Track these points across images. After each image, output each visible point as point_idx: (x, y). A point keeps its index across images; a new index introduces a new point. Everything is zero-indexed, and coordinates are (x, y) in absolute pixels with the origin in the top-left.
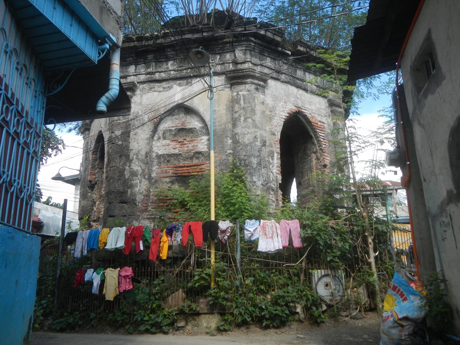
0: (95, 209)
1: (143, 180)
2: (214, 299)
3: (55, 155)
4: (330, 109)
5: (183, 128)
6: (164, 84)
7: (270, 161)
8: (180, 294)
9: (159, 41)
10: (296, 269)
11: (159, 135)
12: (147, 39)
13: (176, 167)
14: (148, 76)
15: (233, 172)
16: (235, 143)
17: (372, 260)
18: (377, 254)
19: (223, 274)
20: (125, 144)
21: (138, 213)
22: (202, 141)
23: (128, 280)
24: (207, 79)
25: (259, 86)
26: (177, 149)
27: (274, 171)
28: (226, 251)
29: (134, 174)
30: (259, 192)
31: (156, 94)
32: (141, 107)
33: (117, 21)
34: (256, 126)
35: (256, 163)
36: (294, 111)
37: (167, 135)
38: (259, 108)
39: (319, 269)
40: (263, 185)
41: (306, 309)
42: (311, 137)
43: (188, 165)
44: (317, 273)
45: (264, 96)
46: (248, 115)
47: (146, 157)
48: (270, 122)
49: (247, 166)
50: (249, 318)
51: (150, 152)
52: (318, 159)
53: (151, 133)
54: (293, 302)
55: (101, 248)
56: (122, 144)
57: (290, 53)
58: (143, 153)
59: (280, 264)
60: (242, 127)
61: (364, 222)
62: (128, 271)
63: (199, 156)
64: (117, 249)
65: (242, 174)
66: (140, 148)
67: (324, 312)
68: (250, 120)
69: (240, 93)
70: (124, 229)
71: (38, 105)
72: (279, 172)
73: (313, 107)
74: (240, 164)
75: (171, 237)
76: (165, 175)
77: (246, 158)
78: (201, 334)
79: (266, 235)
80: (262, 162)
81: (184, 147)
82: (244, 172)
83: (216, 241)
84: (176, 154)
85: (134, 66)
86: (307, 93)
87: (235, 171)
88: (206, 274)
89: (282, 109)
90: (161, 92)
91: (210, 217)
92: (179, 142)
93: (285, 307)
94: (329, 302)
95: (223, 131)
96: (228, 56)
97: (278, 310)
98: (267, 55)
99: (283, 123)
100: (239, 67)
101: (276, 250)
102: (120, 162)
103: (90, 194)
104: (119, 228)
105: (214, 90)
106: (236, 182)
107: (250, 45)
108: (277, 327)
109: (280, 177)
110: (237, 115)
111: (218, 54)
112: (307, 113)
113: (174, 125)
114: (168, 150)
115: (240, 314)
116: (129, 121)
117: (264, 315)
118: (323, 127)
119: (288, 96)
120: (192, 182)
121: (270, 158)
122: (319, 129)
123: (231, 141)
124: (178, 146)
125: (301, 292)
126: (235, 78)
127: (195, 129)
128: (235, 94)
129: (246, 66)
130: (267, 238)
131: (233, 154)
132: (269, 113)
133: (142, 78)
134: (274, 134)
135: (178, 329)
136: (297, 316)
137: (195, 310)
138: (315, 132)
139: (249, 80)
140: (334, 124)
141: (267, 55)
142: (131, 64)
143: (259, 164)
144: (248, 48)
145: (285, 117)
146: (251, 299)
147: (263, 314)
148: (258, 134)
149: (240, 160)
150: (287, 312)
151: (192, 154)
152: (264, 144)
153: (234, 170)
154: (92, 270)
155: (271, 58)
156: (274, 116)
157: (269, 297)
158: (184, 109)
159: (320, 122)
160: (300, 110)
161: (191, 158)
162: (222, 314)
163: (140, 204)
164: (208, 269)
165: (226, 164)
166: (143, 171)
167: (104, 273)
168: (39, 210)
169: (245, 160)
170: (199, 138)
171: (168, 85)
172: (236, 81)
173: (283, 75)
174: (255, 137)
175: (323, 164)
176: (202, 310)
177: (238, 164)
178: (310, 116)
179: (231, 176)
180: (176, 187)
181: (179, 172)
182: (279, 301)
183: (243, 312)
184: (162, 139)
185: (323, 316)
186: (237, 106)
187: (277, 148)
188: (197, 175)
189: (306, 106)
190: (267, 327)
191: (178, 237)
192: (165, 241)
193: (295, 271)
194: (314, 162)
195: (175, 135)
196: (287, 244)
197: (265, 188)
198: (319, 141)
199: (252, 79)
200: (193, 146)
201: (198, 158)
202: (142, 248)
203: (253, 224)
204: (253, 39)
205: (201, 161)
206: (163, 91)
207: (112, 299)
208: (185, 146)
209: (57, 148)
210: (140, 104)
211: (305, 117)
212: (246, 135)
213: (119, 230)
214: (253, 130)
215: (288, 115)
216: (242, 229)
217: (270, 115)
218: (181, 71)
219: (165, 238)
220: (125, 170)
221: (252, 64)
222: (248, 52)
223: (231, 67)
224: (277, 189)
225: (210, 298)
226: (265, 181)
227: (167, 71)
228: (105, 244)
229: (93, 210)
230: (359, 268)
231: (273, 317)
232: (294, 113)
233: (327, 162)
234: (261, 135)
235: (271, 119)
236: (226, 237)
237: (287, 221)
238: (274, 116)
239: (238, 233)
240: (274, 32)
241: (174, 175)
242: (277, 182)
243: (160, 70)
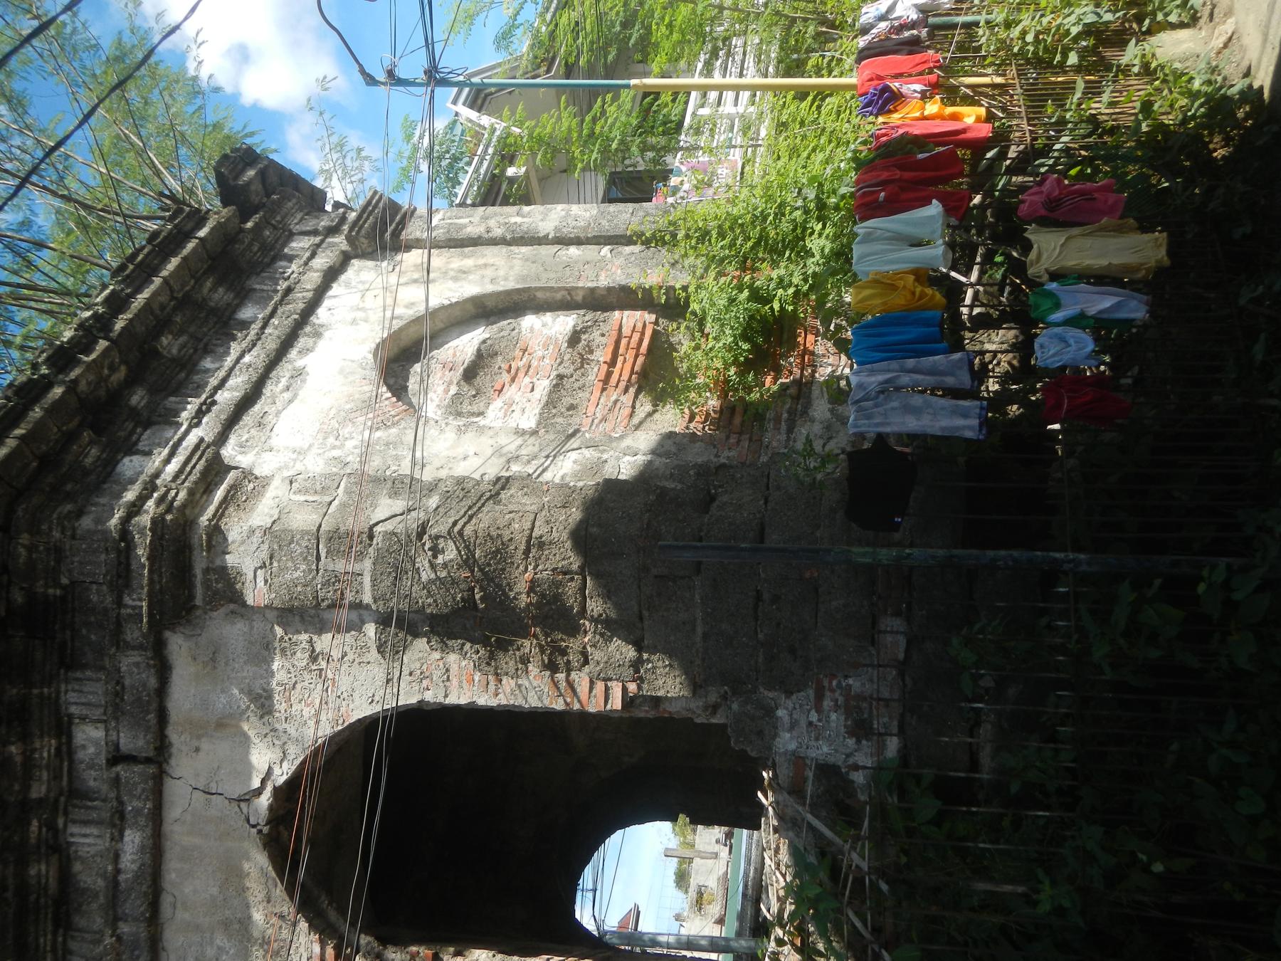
5: (466, 371)
9: (119, 325)
14: (205, 420)
26: (537, 383)
66: (489, 451)
76: (627, 411)
84: (556, 386)
113: (440, 389)
114: (528, 405)
127: (484, 342)
181: (625, 377)
200: (546, 347)
205: (603, 340)
207: (1160, 237)
208: (534, 363)
218: (259, 339)
241: (632, 390)
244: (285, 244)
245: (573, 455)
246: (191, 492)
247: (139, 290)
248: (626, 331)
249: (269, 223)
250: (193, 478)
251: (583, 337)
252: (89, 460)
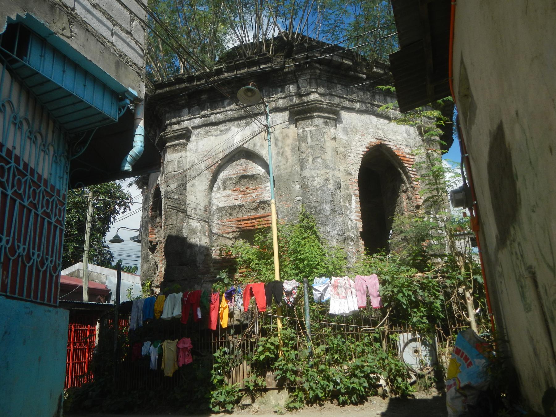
0: (158, 274)
1: (203, 237)
2: (281, 372)
3: (123, 213)
6: (221, 127)
7: (346, 206)
8: (245, 367)
10: (377, 333)
11: (218, 184)
12: (199, 78)
13: (239, 221)
15: (303, 222)
16: (304, 188)
17: (472, 319)
18: (478, 311)
19: (291, 342)
20: (181, 198)
21: (200, 276)
22: (267, 188)
23: (187, 353)
24: (262, 118)
26: (239, 200)
27: (352, 218)
28: (294, 316)
29: (193, 231)
30: (335, 244)
31: (212, 138)
32: (197, 155)
33: (138, 73)
34: (327, 167)
35: (329, 209)
36: (374, 144)
37: (228, 184)
38: (330, 145)
39: (405, 332)
40: (339, 235)
41: (391, 380)
42: (400, 174)
43: (253, 217)
44: (402, 338)
45: (335, 130)
46: (317, 154)
47: (206, 211)
48: (345, 160)
49: (319, 214)
50: (322, 393)
51: (210, 206)
52: (409, 199)
53: (209, 183)
54: (374, 373)
55: (158, 318)
56: (178, 199)
57: (365, 76)
58: (201, 207)
59: (356, 329)
60: (311, 169)
61: (460, 274)
62: (187, 343)
63: (264, 206)
64: (173, 318)
65: (312, 224)
67: (412, 384)
68: (319, 160)
69: (306, 129)
70: (181, 294)
71: (60, 171)
72: (359, 218)
73: (399, 138)
74: (311, 212)
75: (231, 302)
76: (227, 231)
77: (317, 205)
78: (269, 412)
79: (338, 294)
80: (337, 208)
81: (247, 197)
82: (316, 222)
83: (281, 304)
85: (187, 109)
87: (305, 221)
88: (272, 344)
89: (358, 144)
90: (218, 135)
91: (274, 278)
92: (241, 192)
93: (364, 379)
94: (419, 372)
95: (289, 176)
96: (292, 89)
97: (355, 383)
98: (336, 82)
99: (361, 159)
100: (305, 99)
101: (350, 312)
102: (177, 218)
103: (151, 256)
104: (176, 294)
105: (271, 130)
106: (306, 235)
108: (356, 404)
109: (360, 225)
110: (304, 156)
111: (279, 86)
112: (392, 145)
113: (235, 172)
114: (229, 201)
115: (311, 388)
116: (184, 172)
117: (339, 390)
118: (412, 160)
119: (366, 127)
120: (258, 237)
121: (347, 202)
122: (408, 162)
123: (299, 186)
124: (240, 196)
125: (384, 360)
126: (300, 114)
128: (301, 131)
129: (313, 97)
130: (340, 298)
131: (303, 203)
132: (343, 150)
133: (197, 121)
134: (350, 174)
135: (244, 407)
136: (381, 389)
137: (262, 385)
138: (404, 168)
139: (316, 114)
141: (336, 82)
142: (183, 107)
143: (333, 210)
144: (313, 77)
145: (363, 153)
146: (322, 371)
147: (338, 387)
148: (330, 175)
149: (311, 208)
150: (366, 385)
151: (256, 204)
152: (338, 186)
153: (304, 220)
154: (150, 343)
155: (342, 85)
157: (345, 367)
158: (243, 153)
159: (409, 154)
160: (382, 142)
161: (256, 209)
162: (291, 390)
163: (201, 266)
164: (273, 337)
165: (294, 213)
166: (203, 227)
167: (161, 346)
168: (106, 276)
169: (316, 207)
170: (264, 185)
171: (225, 127)
172: (301, 116)
173: (358, 103)
174: (327, 179)
175: (415, 205)
176: (270, 385)
177: (308, 213)
178: (396, 148)
179: (301, 227)
180: (241, 242)
181: (243, 226)
182: (356, 372)
183: (314, 386)
184: (222, 189)
185: (410, 389)
186: (303, 144)
187: (355, 190)
188: (263, 228)
189: (389, 137)
190: (343, 404)
191: (239, 300)
192: (224, 307)
193: (377, 335)
194: (405, 203)
195: (236, 184)
196: (364, 304)
197: (343, 238)
198: (408, 178)
199: (319, 112)
200: (257, 195)
201: (263, 208)
202: (200, 316)
203: (323, 283)
204: (317, 65)
206: (221, 134)
207: (171, 375)
208: (248, 195)
209: (125, 205)
210: (196, 151)
212: (316, 178)
213: (175, 297)
214: (323, 171)
215: (366, 150)
216: (310, 289)
217: (345, 151)
219: (224, 303)
220: (182, 227)
221: (319, 94)
222: (313, 81)
223: (296, 100)
224: (357, 238)
225: (277, 372)
226: (342, 230)
227: (223, 112)
228: (161, 313)
229: (155, 274)
230: (456, 329)
231: (351, 392)
232: (374, 147)
233: (420, 202)
234: (334, 176)
235: (345, 156)
236: (292, 300)
237: (363, 277)
239: (306, 293)
240: (342, 55)
241: (238, 230)
242: (357, 230)
243: (215, 111)
244: (290, 84)
245: (199, 225)
246: (171, 137)
247: (227, 72)
248: (266, 219)
249: (295, 73)
250: (175, 134)
251: (266, 205)
252: (180, 103)
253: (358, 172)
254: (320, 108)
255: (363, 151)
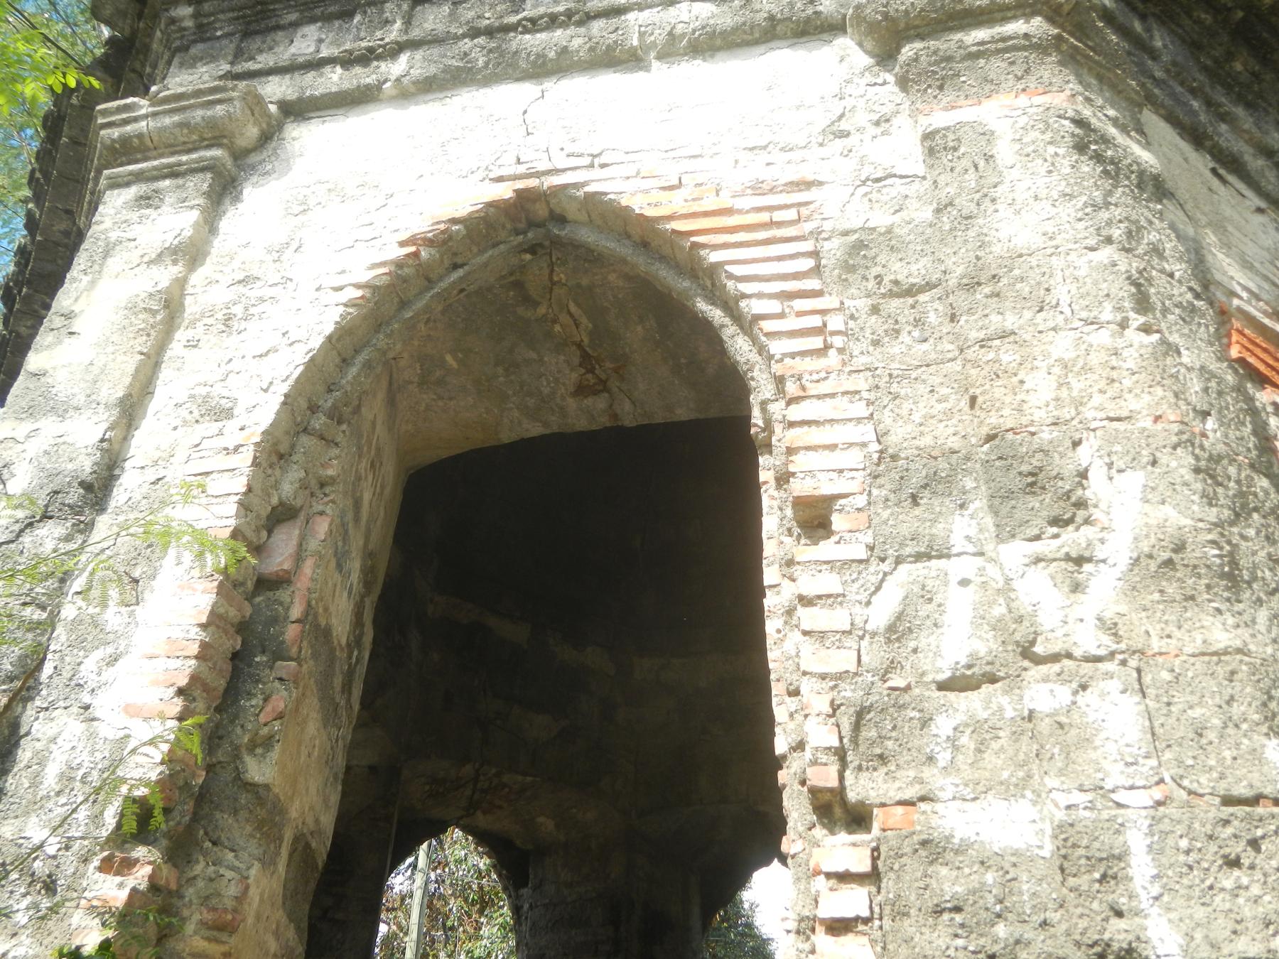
4: (890, 78)
25: (174, 175)
36: (463, 210)
86: (647, 68)
98: (293, 17)
107: (173, 21)
118: (791, 214)
140: (935, 145)
141: (293, 17)
145: (366, 276)
155: (327, 19)
156: (262, 300)
173: (404, 58)
211: (606, 213)
238: (262, 300)
253: (285, 388)
254: (125, 141)
255: (374, 266)
